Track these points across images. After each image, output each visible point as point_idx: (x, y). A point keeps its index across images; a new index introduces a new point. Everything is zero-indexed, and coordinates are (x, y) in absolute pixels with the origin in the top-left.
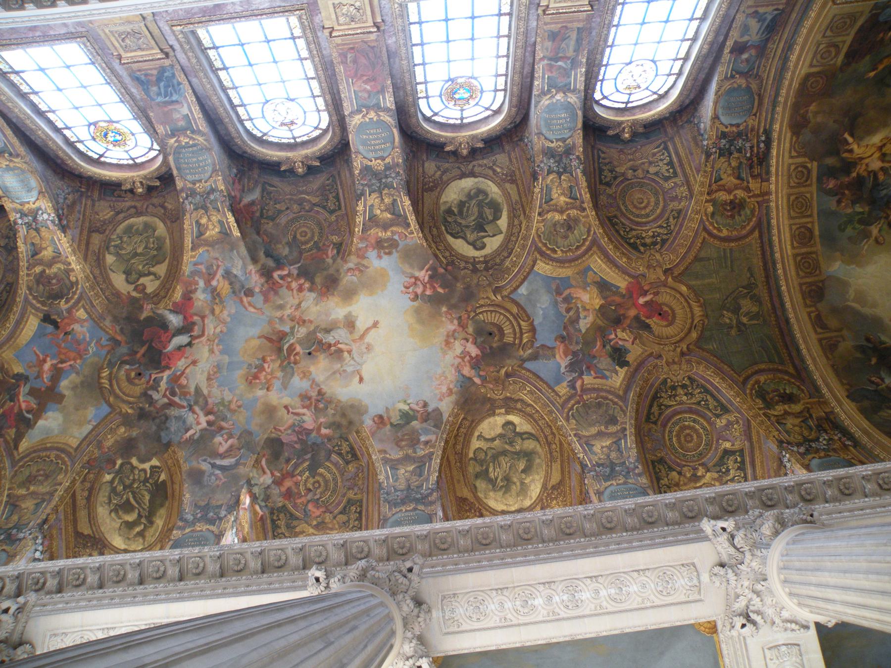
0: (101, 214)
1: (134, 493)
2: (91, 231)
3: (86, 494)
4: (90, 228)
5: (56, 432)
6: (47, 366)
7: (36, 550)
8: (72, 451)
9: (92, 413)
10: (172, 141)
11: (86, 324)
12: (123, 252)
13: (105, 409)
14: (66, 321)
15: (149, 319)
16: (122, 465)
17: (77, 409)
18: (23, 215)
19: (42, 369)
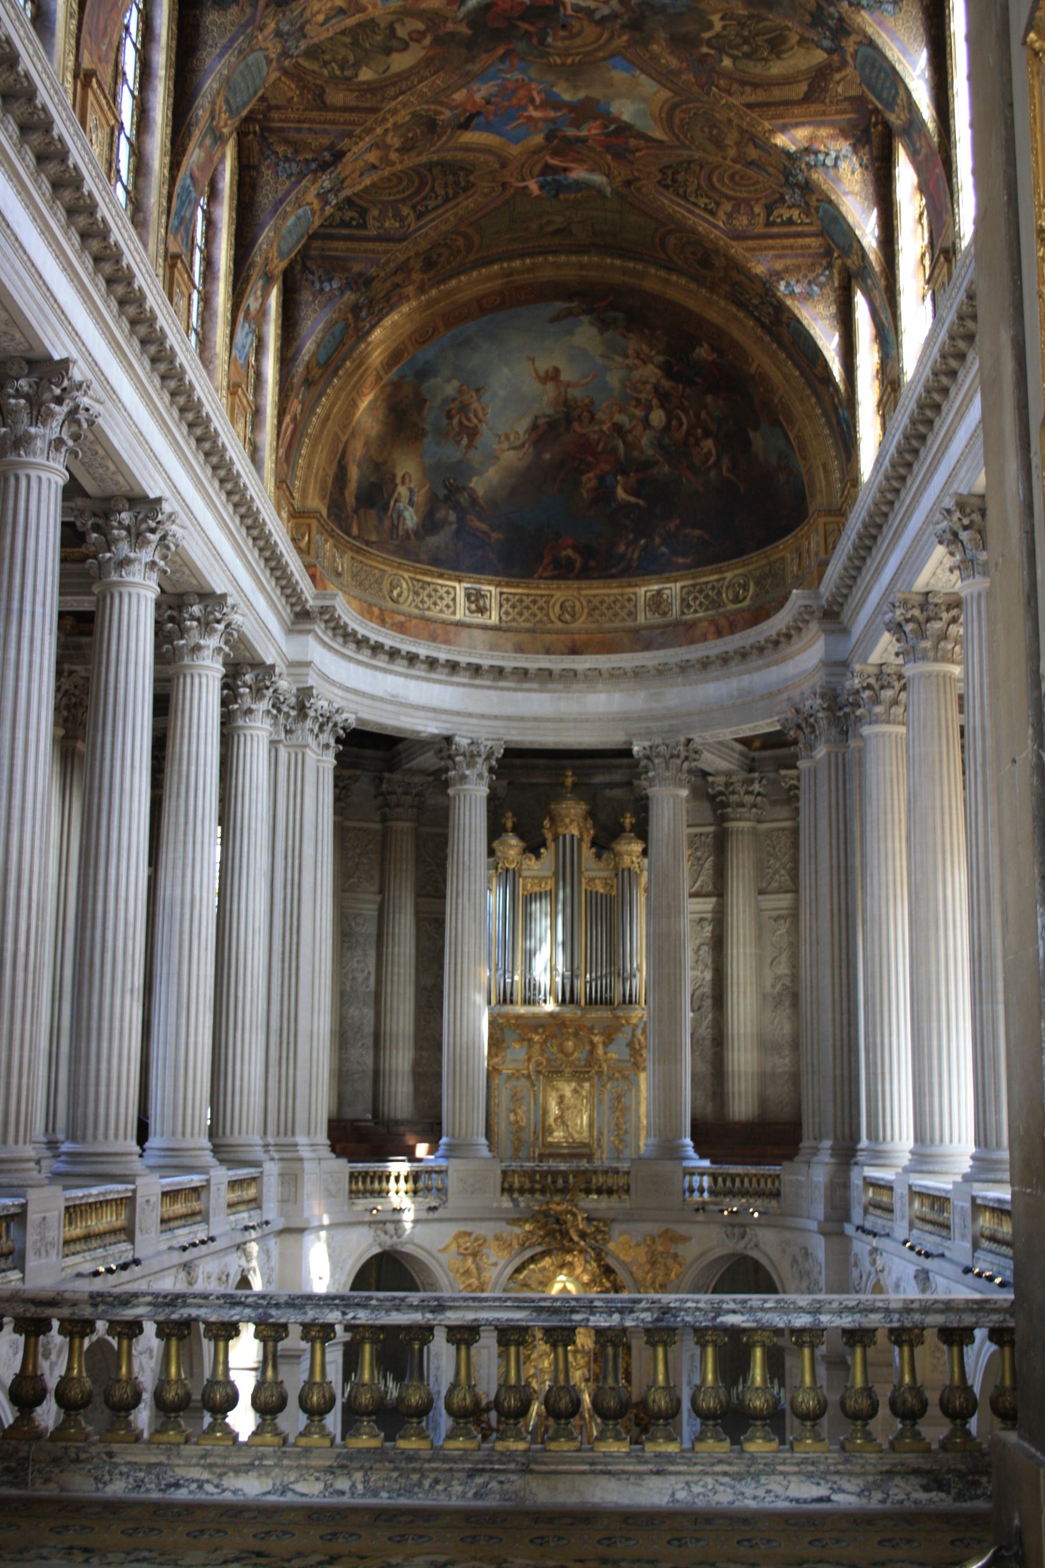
0: (290, 94)
1: (758, 35)
2: (324, 107)
3: (748, 89)
4: (319, 109)
5: (642, 106)
7: (824, 164)
8: (677, 99)
11: (475, 88)
12: (351, 59)
14: (469, 107)
15: (468, 26)
16: (710, 45)
19: (540, 119)
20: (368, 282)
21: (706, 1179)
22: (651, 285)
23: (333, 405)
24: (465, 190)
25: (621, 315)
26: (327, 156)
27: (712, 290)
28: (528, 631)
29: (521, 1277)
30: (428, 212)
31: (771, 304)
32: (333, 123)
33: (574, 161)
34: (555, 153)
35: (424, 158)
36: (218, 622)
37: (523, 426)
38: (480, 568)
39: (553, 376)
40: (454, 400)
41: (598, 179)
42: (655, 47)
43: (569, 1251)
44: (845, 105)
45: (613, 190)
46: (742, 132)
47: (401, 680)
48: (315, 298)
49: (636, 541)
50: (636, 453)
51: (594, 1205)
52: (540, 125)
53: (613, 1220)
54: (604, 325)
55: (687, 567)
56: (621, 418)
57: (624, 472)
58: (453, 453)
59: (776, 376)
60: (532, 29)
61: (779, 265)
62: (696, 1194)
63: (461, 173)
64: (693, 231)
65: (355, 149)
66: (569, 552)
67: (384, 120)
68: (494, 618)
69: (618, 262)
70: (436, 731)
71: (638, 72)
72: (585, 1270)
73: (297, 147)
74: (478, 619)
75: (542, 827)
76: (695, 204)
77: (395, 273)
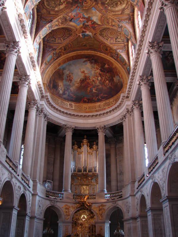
1: (114, 3)
2: (50, 14)
3: (113, 12)
5: (97, 18)
6: (81, 20)
9: (94, 11)
10: (34, 3)
12: (54, 7)
13: (93, 8)
16: (107, 5)
17: (92, 14)
18: (50, 29)
20: (56, 49)
21: (109, 195)
22: (98, 55)
23: (50, 69)
24: (71, 35)
25: (94, 61)
26: (50, 21)
27: (107, 55)
28: (79, 110)
29: (76, 214)
30: (65, 39)
31: (117, 54)
32: (51, 16)
33: (87, 30)
34: (84, 28)
35: (64, 26)
36: (28, 79)
37: (79, 80)
38: (72, 101)
39: (83, 72)
40: (68, 75)
41: (90, 34)
42: (99, 5)
43: (85, 209)
44: (127, 15)
45: (93, 37)
46: (112, 19)
47: (58, 115)
48: (47, 51)
49: (96, 98)
50: (96, 84)
51: (89, 201)
52: (82, 22)
53: (92, 203)
54: (91, 63)
55: (104, 100)
56: (94, 79)
57: (94, 88)
58: (68, 83)
59: (117, 66)
60: (81, 1)
61: (118, 48)
62: (107, 198)
63: (70, 32)
64: (105, 43)
65: (54, 20)
66: (86, 100)
67: (59, 16)
68: (74, 108)
69: (93, 52)
70: (64, 124)
71: (96, 10)
72: (87, 213)
73: (46, 20)
74: (71, 108)
75: (81, 144)
76: (105, 38)
77: (60, 49)
